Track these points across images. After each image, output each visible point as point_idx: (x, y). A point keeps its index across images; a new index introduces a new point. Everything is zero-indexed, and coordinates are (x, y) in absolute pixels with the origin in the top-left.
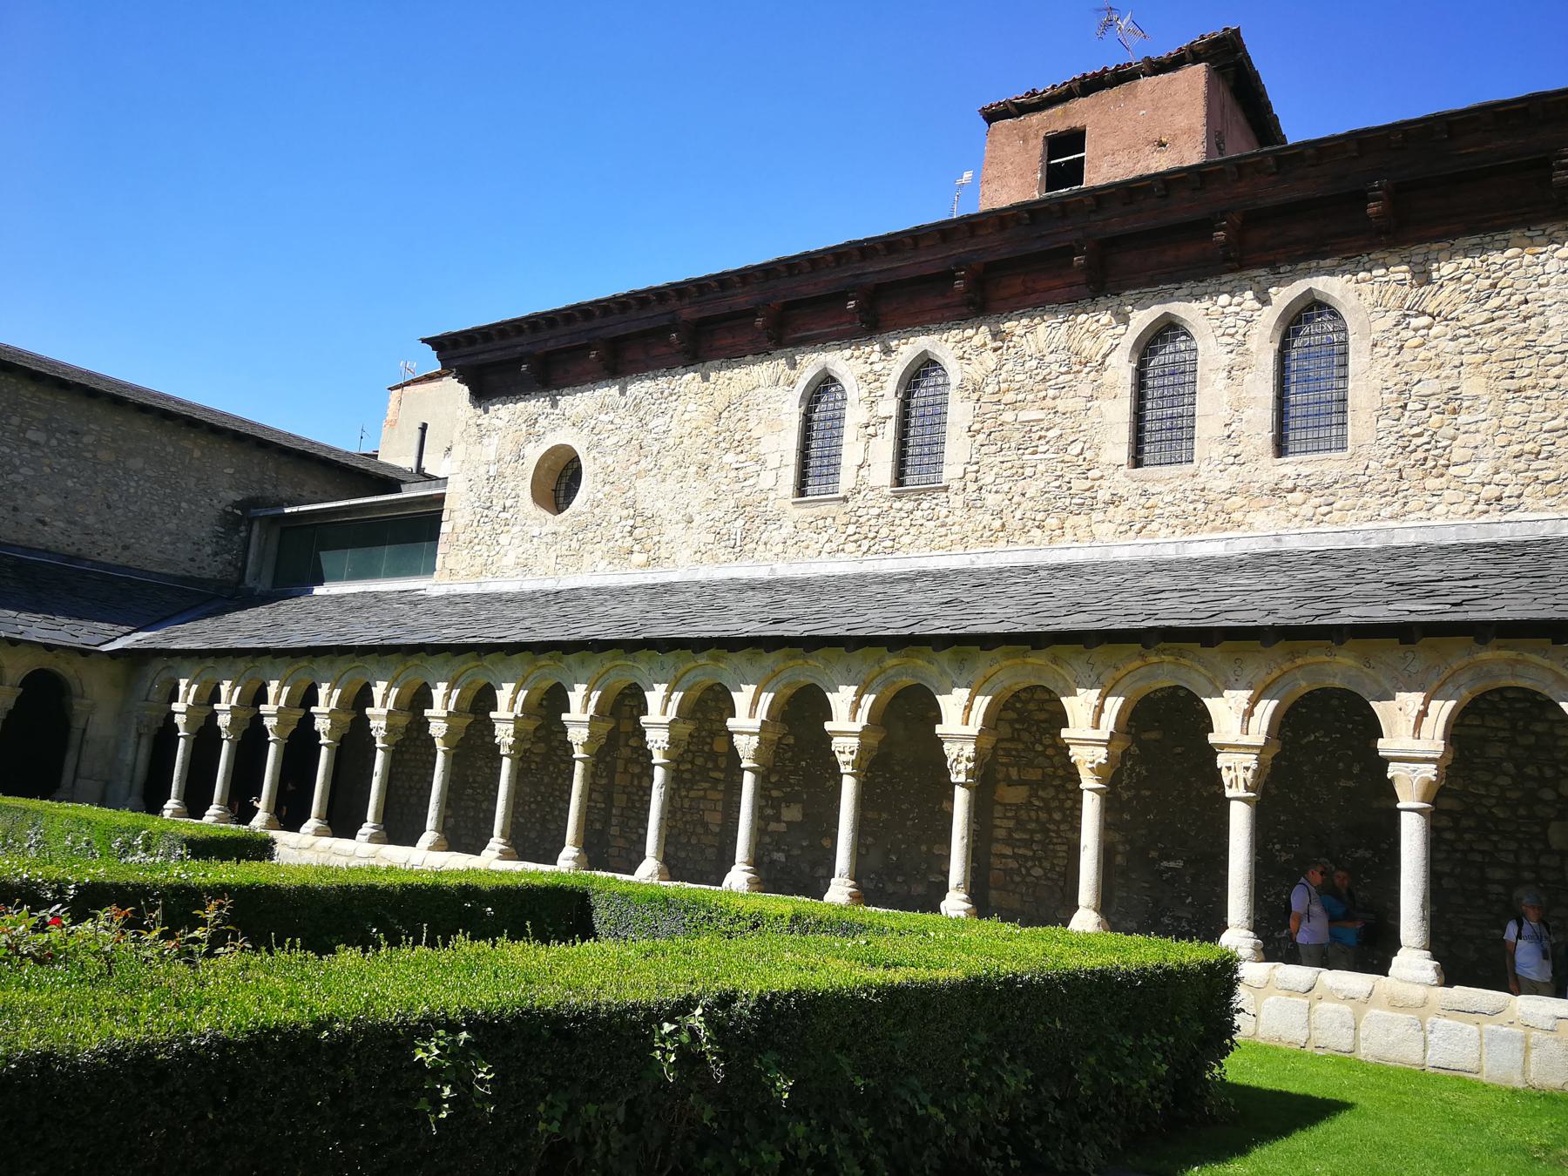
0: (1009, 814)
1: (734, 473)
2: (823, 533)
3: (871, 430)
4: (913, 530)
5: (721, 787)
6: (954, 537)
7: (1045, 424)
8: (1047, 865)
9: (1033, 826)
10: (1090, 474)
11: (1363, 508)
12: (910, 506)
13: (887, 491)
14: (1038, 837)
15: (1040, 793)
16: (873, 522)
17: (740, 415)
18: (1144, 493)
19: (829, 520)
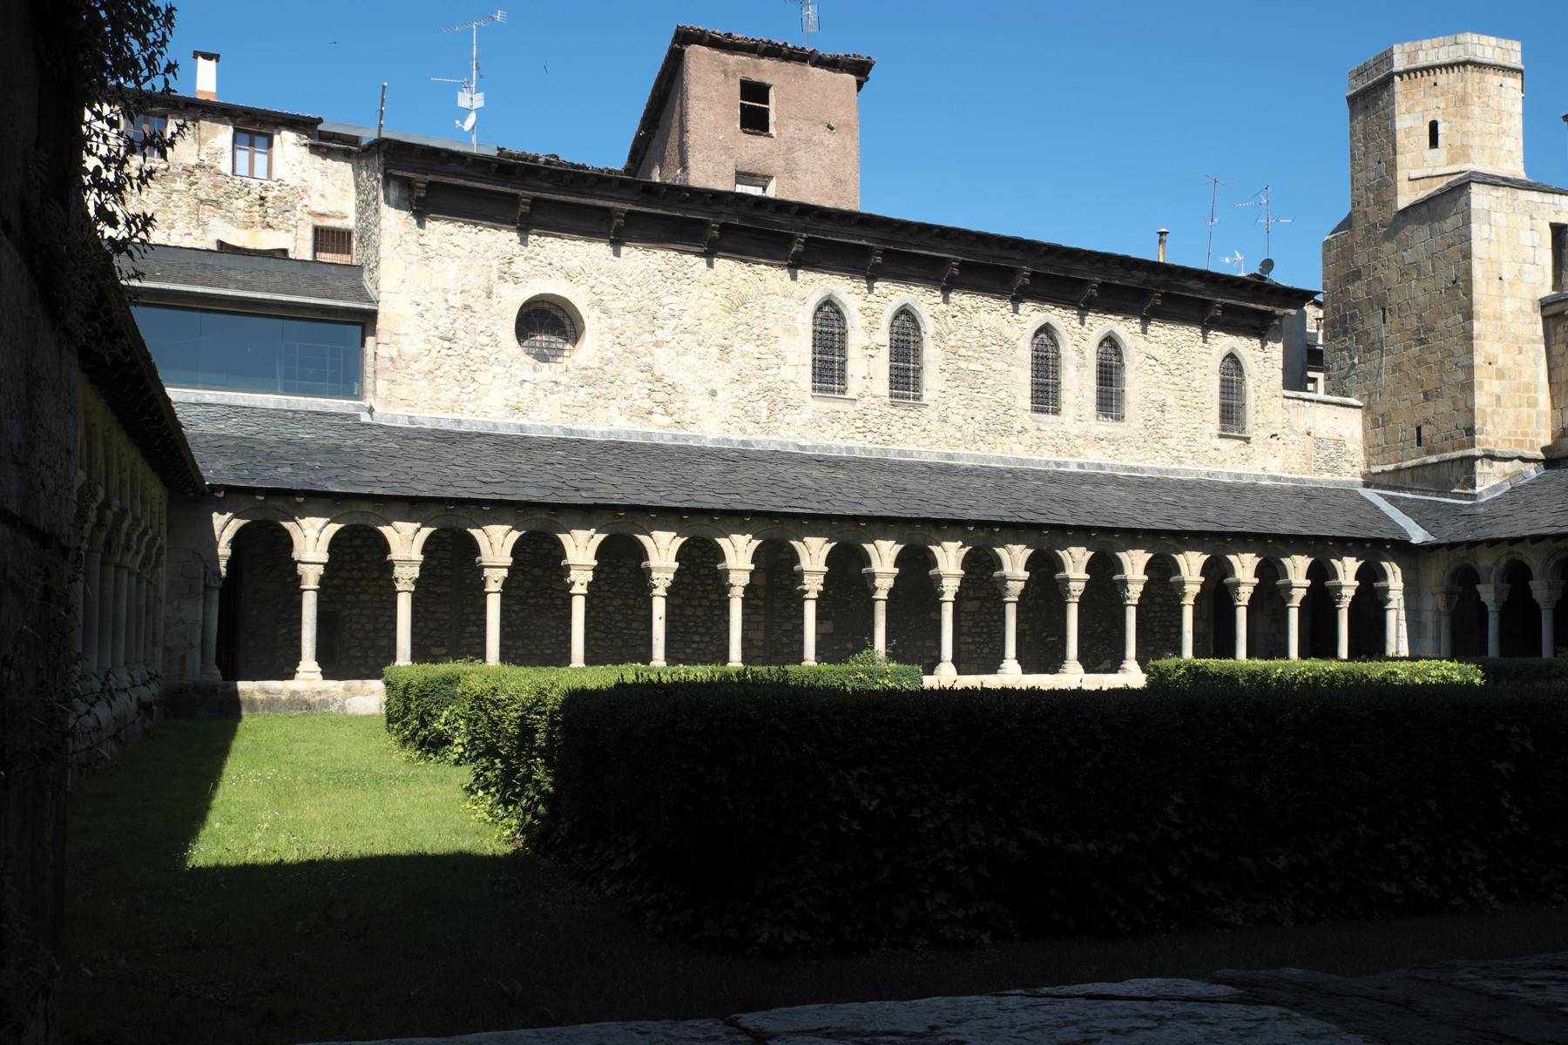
0: (970, 618)
1: (756, 362)
2: (836, 423)
3: (870, 352)
4: (904, 431)
5: (762, 612)
6: (932, 440)
7: (985, 375)
8: (991, 646)
9: (983, 624)
10: (1010, 412)
11: (1131, 453)
12: (903, 413)
13: (887, 400)
14: (985, 630)
15: (986, 604)
16: (875, 420)
17: (757, 313)
18: (1038, 429)
19: (842, 415)
